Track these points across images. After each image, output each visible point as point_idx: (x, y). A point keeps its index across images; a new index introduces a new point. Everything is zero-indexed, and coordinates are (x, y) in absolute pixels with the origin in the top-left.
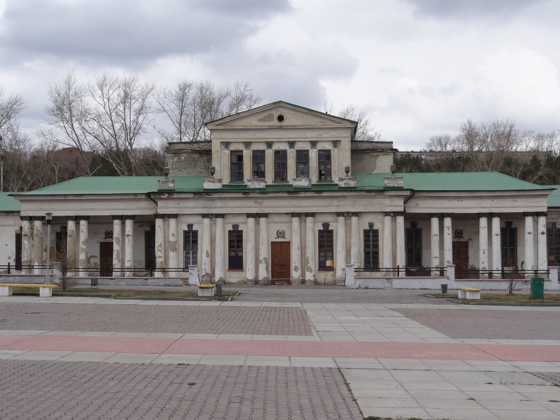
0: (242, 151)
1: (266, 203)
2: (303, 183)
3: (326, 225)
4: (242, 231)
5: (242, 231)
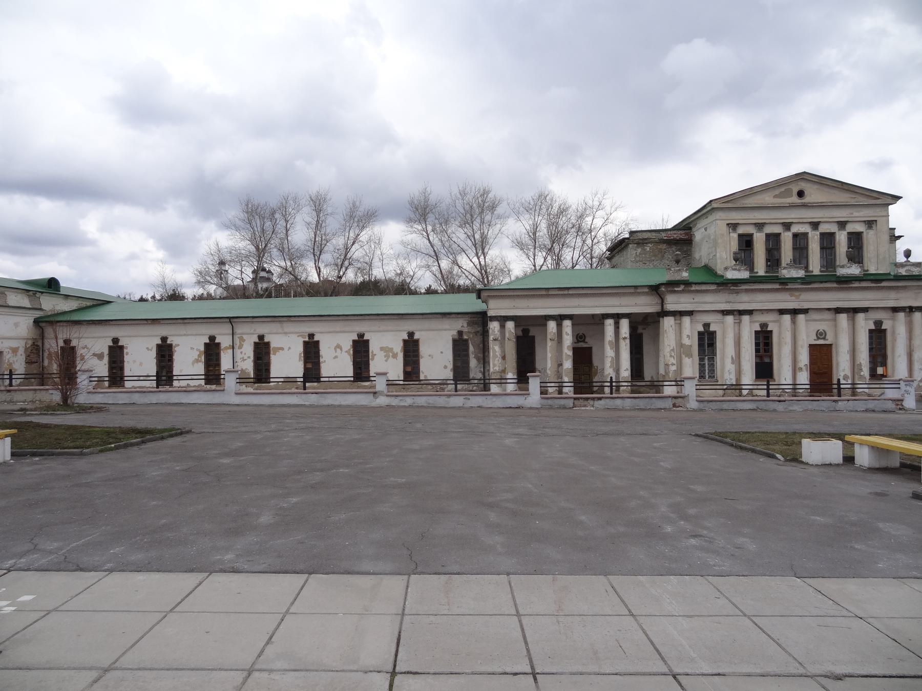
0: (751, 235)
1: (805, 296)
2: (855, 270)
3: (878, 323)
4: (771, 331)
5: (771, 331)
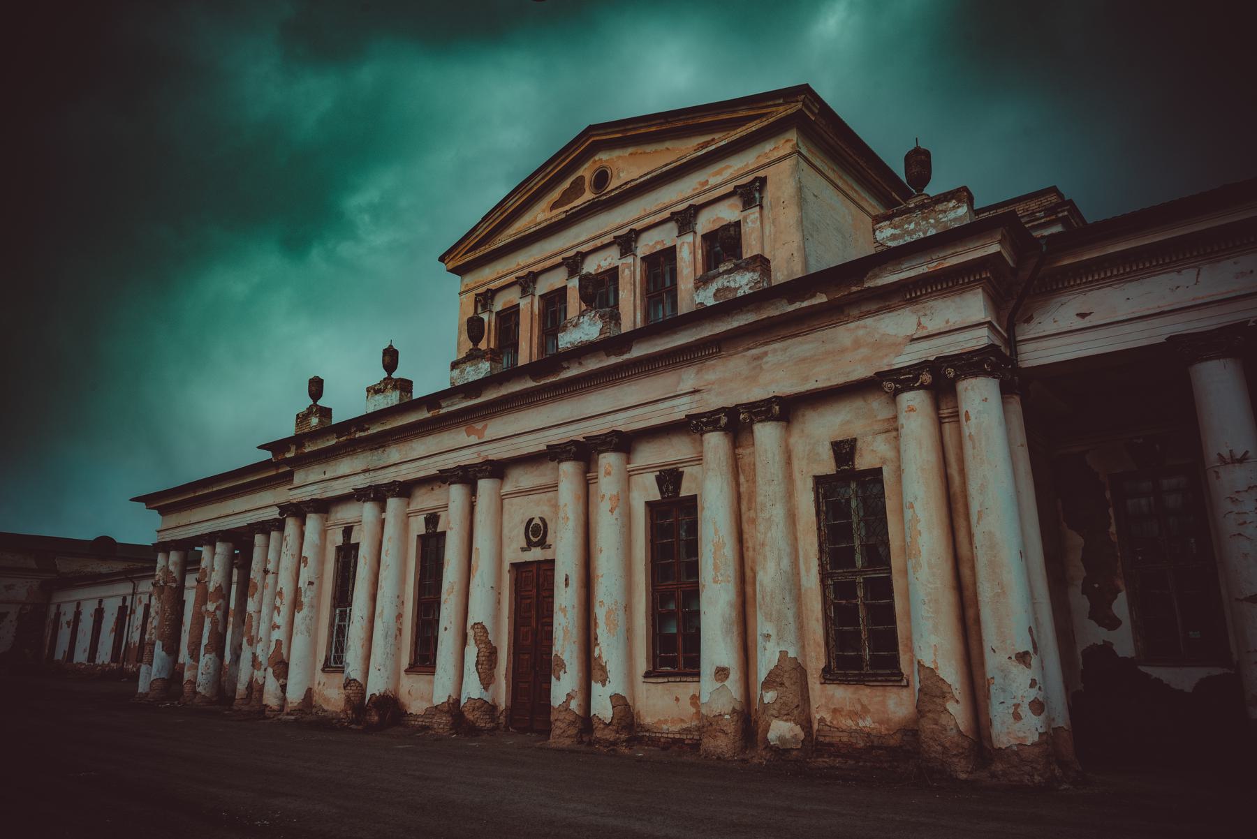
1: (497, 427)
